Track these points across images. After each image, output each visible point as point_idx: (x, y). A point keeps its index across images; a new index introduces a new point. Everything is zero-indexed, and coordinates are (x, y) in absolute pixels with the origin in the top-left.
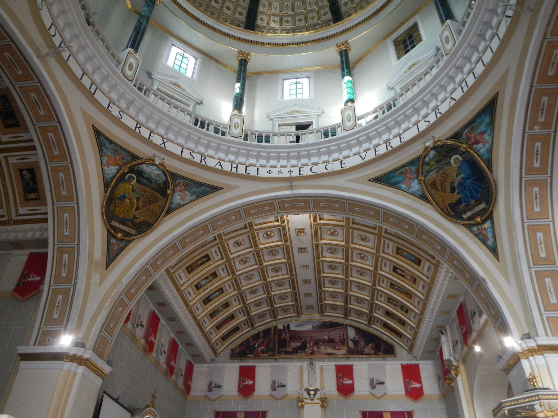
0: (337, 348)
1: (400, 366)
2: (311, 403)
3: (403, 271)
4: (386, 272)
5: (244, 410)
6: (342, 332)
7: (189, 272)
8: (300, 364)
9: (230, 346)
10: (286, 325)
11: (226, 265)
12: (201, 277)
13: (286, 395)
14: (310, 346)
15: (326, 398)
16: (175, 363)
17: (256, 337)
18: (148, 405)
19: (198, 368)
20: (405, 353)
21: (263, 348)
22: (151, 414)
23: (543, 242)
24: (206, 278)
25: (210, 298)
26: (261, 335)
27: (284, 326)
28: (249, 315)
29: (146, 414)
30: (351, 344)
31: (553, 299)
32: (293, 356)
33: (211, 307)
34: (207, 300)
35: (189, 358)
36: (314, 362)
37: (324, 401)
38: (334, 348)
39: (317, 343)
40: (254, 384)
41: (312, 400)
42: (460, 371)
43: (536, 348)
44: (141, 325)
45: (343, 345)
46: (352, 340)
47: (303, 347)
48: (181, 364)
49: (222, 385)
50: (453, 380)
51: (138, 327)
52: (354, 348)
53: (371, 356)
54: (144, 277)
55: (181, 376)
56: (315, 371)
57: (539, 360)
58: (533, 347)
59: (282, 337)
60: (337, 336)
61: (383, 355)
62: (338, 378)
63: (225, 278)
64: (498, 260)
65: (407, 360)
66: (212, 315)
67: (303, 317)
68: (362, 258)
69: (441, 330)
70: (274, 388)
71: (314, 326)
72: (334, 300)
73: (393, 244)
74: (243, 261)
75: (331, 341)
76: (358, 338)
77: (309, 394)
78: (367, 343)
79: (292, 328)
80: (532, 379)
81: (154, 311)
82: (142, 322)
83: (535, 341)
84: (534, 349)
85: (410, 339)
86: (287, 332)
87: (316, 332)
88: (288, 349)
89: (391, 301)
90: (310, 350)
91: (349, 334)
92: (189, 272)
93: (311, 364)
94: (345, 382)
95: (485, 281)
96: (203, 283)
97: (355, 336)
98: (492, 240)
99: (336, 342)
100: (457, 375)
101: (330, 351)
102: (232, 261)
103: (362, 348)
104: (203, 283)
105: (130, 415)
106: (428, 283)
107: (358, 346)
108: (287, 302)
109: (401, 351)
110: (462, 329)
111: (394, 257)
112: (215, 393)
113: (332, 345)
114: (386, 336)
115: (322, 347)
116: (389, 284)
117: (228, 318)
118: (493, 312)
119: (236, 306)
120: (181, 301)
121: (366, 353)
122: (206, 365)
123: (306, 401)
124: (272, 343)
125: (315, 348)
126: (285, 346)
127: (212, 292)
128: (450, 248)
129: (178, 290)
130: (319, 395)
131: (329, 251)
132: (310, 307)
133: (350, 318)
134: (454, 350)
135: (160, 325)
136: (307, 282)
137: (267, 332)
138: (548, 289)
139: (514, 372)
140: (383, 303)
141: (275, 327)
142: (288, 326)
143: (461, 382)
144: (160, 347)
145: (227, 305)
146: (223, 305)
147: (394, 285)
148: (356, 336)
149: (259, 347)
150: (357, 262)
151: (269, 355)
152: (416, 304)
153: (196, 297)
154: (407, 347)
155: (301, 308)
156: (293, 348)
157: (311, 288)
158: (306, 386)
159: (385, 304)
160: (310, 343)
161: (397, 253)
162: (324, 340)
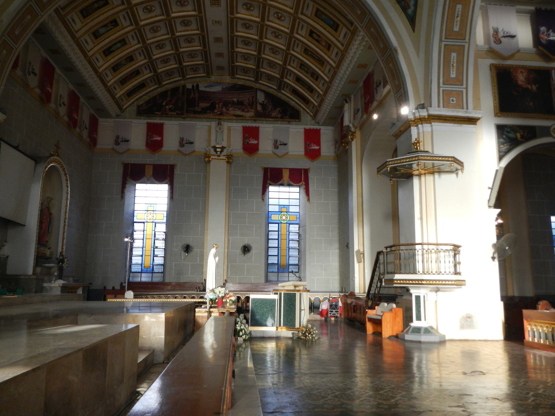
0: (246, 110)
1: (303, 130)
2: (217, 159)
3: (319, 36)
4: (302, 36)
5: (153, 163)
7: (85, 17)
8: (208, 124)
9: (136, 102)
10: (195, 85)
11: (127, 12)
12: (99, 23)
13: (194, 151)
14: (219, 108)
15: (232, 155)
16: (77, 116)
17: (164, 95)
18: (52, 154)
19: (103, 123)
20: (309, 118)
21: (171, 106)
22: (56, 162)
23: (460, 16)
24: (105, 26)
25: (112, 49)
26: (169, 93)
27: (193, 86)
28: (155, 71)
29: (51, 163)
30: (259, 108)
31: (453, 74)
33: (113, 59)
34: (108, 52)
35: (93, 112)
36: (222, 123)
37: (230, 158)
38: (243, 110)
39: (226, 104)
40: (162, 140)
41: (219, 156)
42: (356, 136)
43: (427, 117)
44: (33, 72)
45: (252, 108)
46: (260, 104)
47: (212, 108)
48: (85, 117)
49: (129, 139)
50: (349, 143)
51: (30, 75)
52: (262, 112)
54: (29, 17)
55: (85, 129)
56: (223, 131)
57: (427, 127)
58: (425, 116)
62: (244, 138)
63: (127, 27)
64: (414, 31)
65: (310, 125)
66: (115, 68)
67: (213, 78)
68: (279, 18)
69: (345, 98)
70: (182, 144)
71: (224, 87)
72: (246, 62)
73: (313, 5)
74: (148, 9)
75: (240, 104)
76: (266, 102)
77: (216, 152)
79: (202, 88)
80: (416, 143)
81: (47, 58)
82: (33, 69)
83: (427, 111)
84: (425, 118)
85: (316, 106)
88: (196, 108)
89: (303, 67)
90: (218, 111)
91: (258, 97)
92: (85, 17)
93: (219, 124)
94: (251, 142)
95: (396, 51)
96: (102, 31)
97: (264, 100)
98: (412, 8)
100: (352, 139)
101: (239, 112)
102: (135, 8)
104: (102, 31)
105: (33, 162)
106: (341, 51)
108: (197, 61)
109: (306, 117)
110: (365, 98)
111: (312, 20)
112: (122, 147)
114: (294, 101)
115: (231, 109)
116: (303, 50)
117: (133, 73)
118: (397, 83)
119: (141, 61)
120: (77, 50)
121: (273, 116)
122: (112, 120)
123: (212, 157)
125: (224, 109)
127: (113, 43)
128: (370, 13)
129: (73, 37)
130: (225, 152)
131: (244, 7)
132: (220, 68)
133: (260, 82)
134: (354, 117)
135: (55, 75)
136: (218, 40)
137: (175, 91)
138: (452, 63)
139: (402, 138)
140: (295, 69)
141: (184, 86)
142: (198, 86)
143: (355, 147)
144: (59, 98)
145: (130, 59)
147: (308, 50)
148: (265, 100)
149: (167, 105)
150: (273, 22)
151: (177, 114)
152: (327, 71)
153: (95, 46)
154: (312, 113)
155: (212, 69)
157: (223, 47)
158: (213, 144)
159: (296, 70)
161: (316, 15)
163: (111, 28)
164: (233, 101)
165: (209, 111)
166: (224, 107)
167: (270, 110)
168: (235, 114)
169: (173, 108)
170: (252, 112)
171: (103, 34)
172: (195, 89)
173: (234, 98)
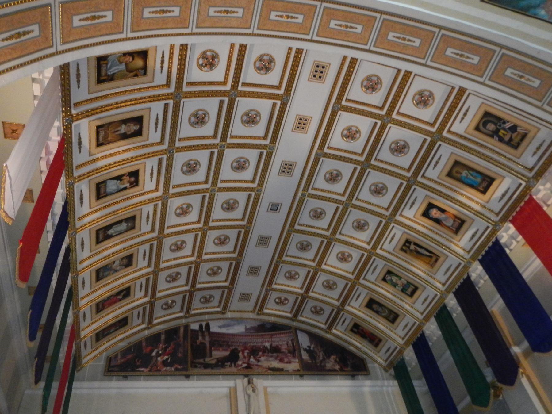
0: (286, 360)
6: (290, 339)
10: (204, 324)
14: (245, 357)
17: (154, 339)
21: (166, 357)
24: (119, 178)
25: (110, 232)
26: (163, 337)
27: (201, 326)
30: (305, 356)
32: (216, 371)
38: (281, 360)
39: (254, 352)
45: (294, 356)
47: (233, 358)
52: (310, 361)
53: (335, 373)
59: (198, 342)
60: (285, 343)
61: (352, 373)
71: (248, 327)
75: (275, 350)
76: (314, 348)
78: (328, 355)
79: (215, 328)
86: (206, 333)
87: (251, 336)
88: (208, 360)
90: (244, 363)
91: (300, 341)
97: (309, 344)
99: (283, 352)
101: (276, 364)
103: (321, 361)
107: (315, 359)
113: (277, 357)
115: (262, 358)
121: (327, 368)
124: (181, 350)
126: (204, 356)
137: (172, 333)
141: (187, 327)
142: (208, 326)
146: (123, 259)
148: (311, 345)
151: (177, 369)
156: (217, 359)
160: (243, 353)
162: (267, 348)
163: (125, 186)
164: (264, 346)
165: (229, 363)
166: (252, 357)
167: (321, 359)
168: (271, 366)
169: (169, 361)
170: (295, 362)
171: (112, 194)
172: (204, 330)
173: (266, 342)
